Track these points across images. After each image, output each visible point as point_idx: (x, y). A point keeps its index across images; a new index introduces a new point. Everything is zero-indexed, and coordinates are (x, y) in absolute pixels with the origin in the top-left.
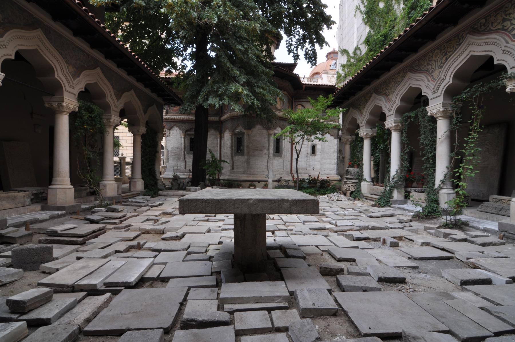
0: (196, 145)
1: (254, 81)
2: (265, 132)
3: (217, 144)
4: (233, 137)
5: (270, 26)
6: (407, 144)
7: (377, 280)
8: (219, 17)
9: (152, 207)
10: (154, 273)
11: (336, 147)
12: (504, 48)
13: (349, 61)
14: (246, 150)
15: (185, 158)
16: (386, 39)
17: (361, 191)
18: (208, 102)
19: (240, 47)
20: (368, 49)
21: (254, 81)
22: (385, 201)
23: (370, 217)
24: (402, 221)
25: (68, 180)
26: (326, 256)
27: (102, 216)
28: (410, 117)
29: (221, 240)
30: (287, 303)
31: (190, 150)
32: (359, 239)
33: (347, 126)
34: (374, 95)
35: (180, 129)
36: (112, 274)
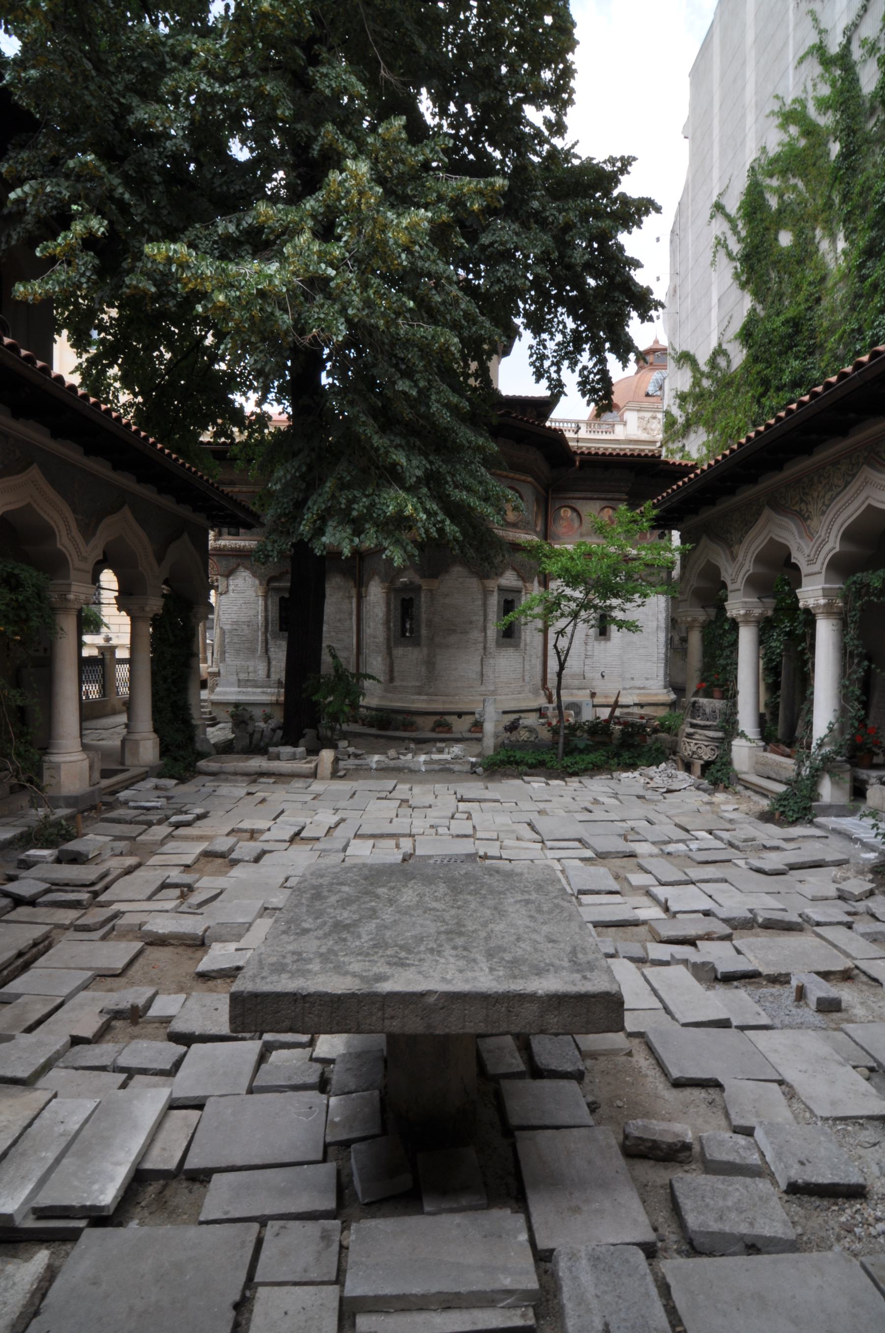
0: (296, 617)
1: (444, 469)
2: (474, 583)
3: (351, 614)
4: (392, 596)
6: (859, 655)
7: (783, 1186)
8: (349, 322)
9: (177, 825)
10: (164, 1158)
11: (662, 616)
13: (696, 383)
14: (424, 632)
15: (267, 650)
16: (797, 332)
17: (730, 763)
18: (324, 539)
20: (748, 356)
21: (444, 469)
22: (794, 807)
23: (759, 871)
24: (846, 895)
26: (642, 1060)
27: (44, 880)
28: (868, 585)
30: (531, 1313)
31: (281, 630)
32: (728, 979)
33: (694, 582)
34: (767, 512)
35: (254, 574)
36: (58, 1161)
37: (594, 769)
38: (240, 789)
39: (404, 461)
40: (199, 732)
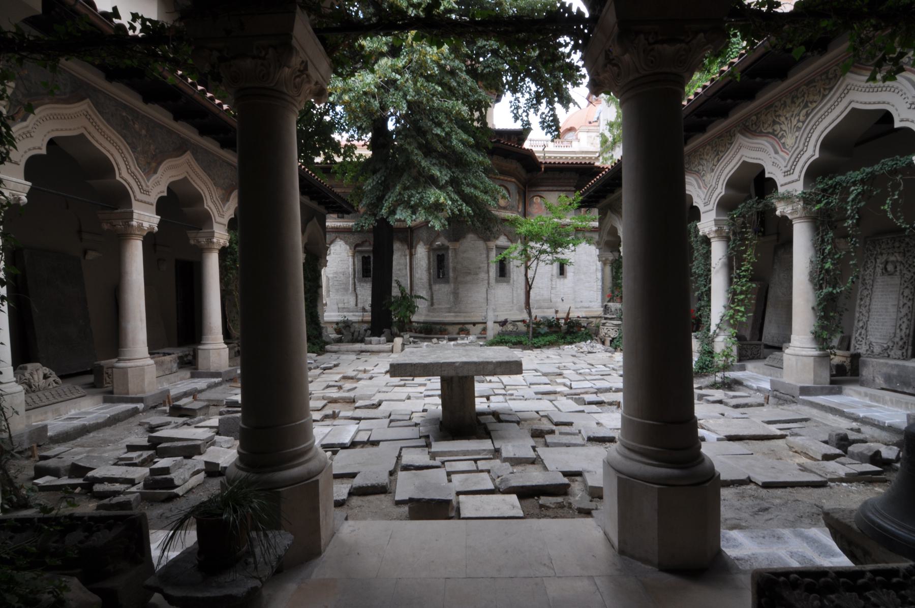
1: (461, 176)
2: (481, 244)
5: (483, 94)
8: (409, 104)
9: (325, 369)
10: (362, 437)
12: (773, 160)
14: (451, 274)
15: (355, 289)
19: (438, 131)
21: (461, 176)
25: (220, 337)
26: (545, 420)
29: (426, 407)
31: (363, 276)
32: (590, 403)
35: (346, 243)
37: (551, 344)
38: (353, 357)
39: (438, 174)
40: (324, 331)
